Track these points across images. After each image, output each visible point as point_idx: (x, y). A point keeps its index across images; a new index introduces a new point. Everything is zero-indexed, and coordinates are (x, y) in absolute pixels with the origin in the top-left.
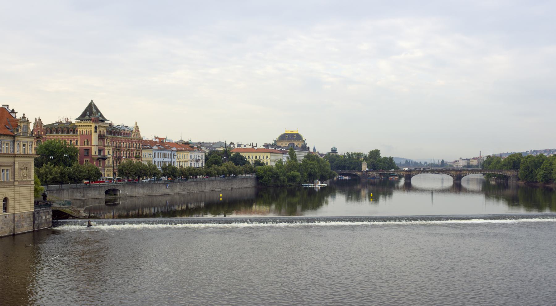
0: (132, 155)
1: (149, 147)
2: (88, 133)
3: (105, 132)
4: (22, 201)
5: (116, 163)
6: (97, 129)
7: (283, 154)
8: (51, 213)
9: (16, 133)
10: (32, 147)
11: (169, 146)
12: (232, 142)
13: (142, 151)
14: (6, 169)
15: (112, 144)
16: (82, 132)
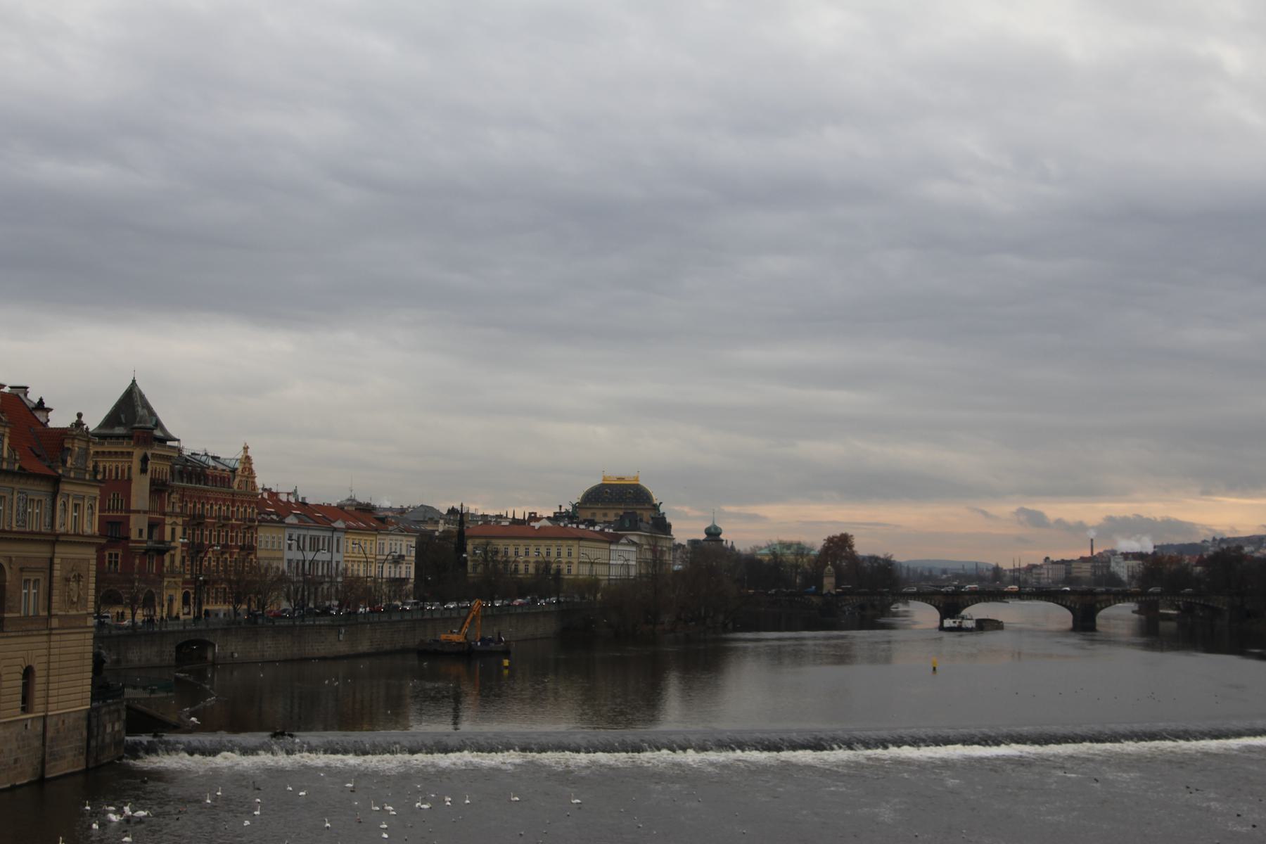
0: (232, 541)
1: (274, 517)
2: (120, 475)
3: (166, 473)
4: (65, 677)
5: (189, 563)
6: (149, 462)
7: (611, 543)
8: (124, 715)
9: (60, 471)
10: (92, 513)
11: (324, 517)
12: (453, 508)
13: (259, 529)
14: (33, 579)
15: (181, 508)
16: (117, 474)
